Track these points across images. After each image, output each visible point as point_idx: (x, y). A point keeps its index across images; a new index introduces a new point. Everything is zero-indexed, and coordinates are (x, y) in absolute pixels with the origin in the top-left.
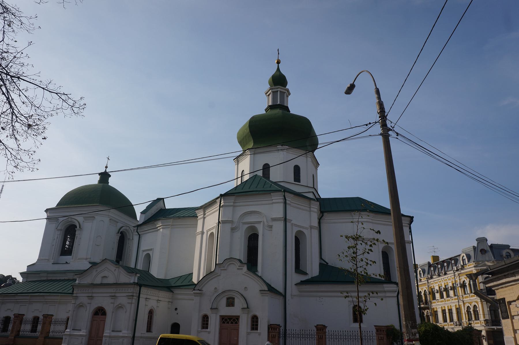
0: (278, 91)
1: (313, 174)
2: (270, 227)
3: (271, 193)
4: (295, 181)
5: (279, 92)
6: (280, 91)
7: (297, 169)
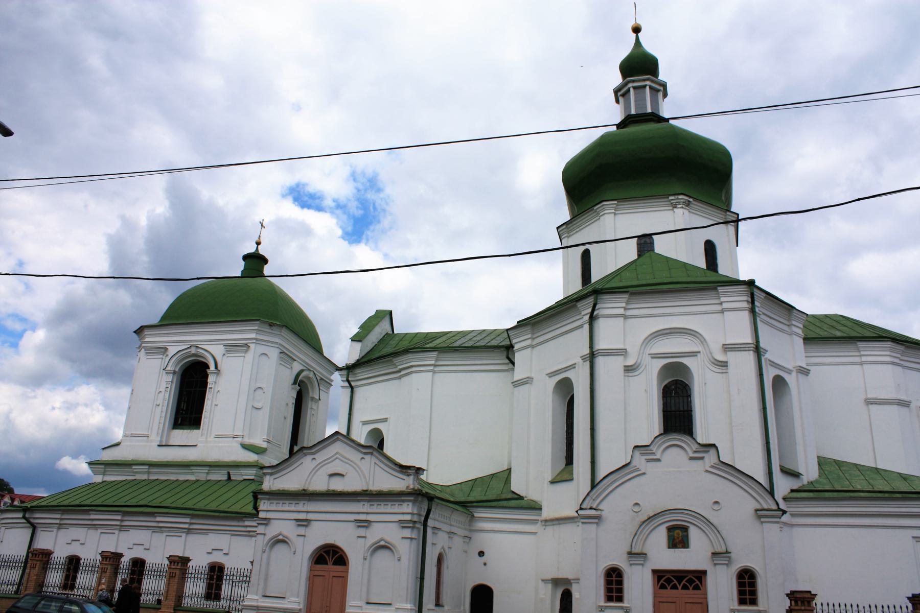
2: (723, 364)
3: (719, 288)
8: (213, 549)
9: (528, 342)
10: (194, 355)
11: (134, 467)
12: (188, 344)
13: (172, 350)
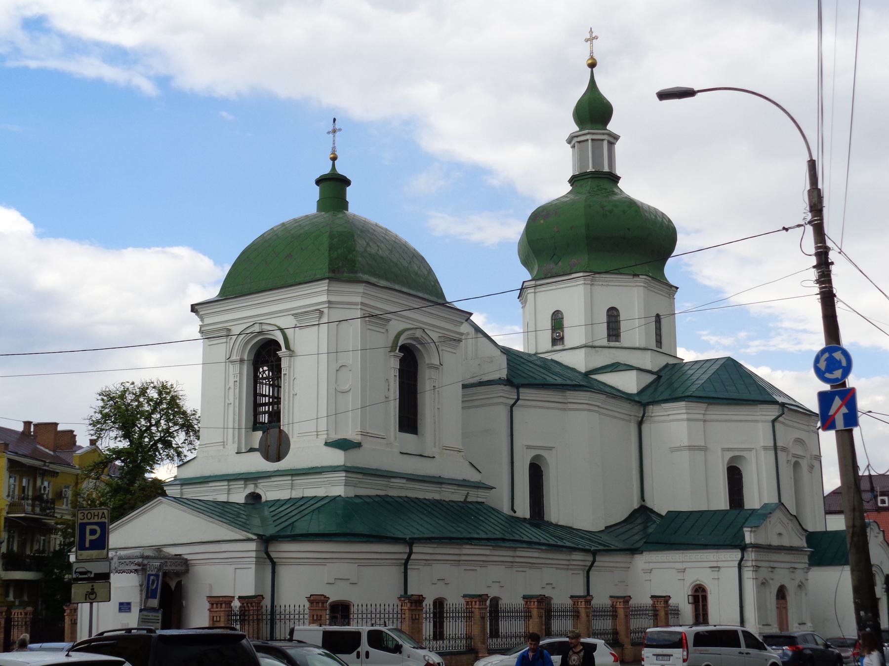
0: (587, 140)
4: (608, 341)
5: (590, 141)
6: (592, 140)
7: (613, 316)
9: (701, 417)
11: (393, 480)
13: (396, 326)
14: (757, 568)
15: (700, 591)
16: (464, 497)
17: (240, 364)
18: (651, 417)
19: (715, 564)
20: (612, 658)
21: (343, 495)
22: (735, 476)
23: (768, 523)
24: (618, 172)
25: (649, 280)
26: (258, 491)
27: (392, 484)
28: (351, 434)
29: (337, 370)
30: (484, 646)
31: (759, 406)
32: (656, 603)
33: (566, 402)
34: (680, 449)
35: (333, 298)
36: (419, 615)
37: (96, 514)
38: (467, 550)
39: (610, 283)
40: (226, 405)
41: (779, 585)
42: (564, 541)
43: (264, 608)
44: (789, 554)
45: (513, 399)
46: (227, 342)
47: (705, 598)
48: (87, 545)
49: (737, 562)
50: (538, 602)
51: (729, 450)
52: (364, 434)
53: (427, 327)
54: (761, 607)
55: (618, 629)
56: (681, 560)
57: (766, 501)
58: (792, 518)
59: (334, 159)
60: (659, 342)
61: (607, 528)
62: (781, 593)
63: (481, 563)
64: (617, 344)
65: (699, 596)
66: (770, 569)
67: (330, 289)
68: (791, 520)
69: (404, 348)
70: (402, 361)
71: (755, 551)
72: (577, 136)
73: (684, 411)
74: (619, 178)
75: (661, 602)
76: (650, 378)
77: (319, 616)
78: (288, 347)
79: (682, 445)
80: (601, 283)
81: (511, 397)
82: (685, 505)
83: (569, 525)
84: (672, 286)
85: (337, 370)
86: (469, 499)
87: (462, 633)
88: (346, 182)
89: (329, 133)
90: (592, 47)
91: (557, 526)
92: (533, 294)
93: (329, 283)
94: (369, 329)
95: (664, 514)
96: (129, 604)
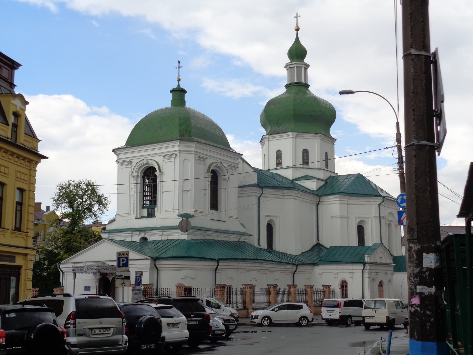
0: (294, 67)
1: (326, 153)
4: (303, 164)
5: (296, 68)
6: (297, 67)
7: (306, 153)
8: (276, 279)
9: (346, 202)
10: (218, 167)
11: (208, 232)
12: (217, 160)
13: (209, 161)
14: (370, 273)
15: (344, 283)
16: (238, 239)
17: (137, 177)
18: (323, 202)
19: (351, 271)
20: (310, 312)
21: (186, 239)
22: (361, 230)
23: (376, 253)
24: (309, 83)
25: (323, 136)
26: (146, 236)
27: (207, 234)
28: (189, 211)
29: (183, 182)
30: (251, 306)
31: (373, 197)
32: (324, 288)
33: (284, 195)
34: (336, 217)
35: (181, 149)
36: (224, 293)
37: (124, 254)
38: (242, 264)
39: (304, 138)
40: (130, 196)
41: (380, 280)
42: (283, 260)
43: (154, 289)
44: (385, 266)
45: (260, 193)
46: (130, 167)
47: (346, 286)
48: (121, 265)
49: (362, 270)
50: (274, 287)
51: (358, 218)
52: (195, 211)
53: (223, 161)
54: (372, 291)
55: (308, 300)
56: (336, 269)
57: (375, 242)
58: (387, 250)
59: (179, 80)
60: (327, 165)
61: (302, 253)
62: (381, 284)
63: (247, 270)
64: (307, 166)
65: (344, 285)
66: (376, 273)
67: (180, 144)
68: (386, 251)
69: (213, 172)
70: (212, 177)
71: (370, 265)
72: (290, 65)
73: (338, 199)
74: (309, 86)
75: (327, 288)
76: (322, 183)
77: (181, 293)
78: (160, 171)
79: (337, 215)
80: (300, 137)
81: (260, 193)
82: (338, 243)
83: (285, 252)
84: (333, 139)
85: (183, 182)
86: (240, 241)
87: (242, 301)
88: (184, 91)
89: (176, 68)
90: (297, 21)
91: (279, 252)
92: (267, 142)
93: (180, 142)
94: (198, 163)
95: (328, 247)
96: (89, 287)
